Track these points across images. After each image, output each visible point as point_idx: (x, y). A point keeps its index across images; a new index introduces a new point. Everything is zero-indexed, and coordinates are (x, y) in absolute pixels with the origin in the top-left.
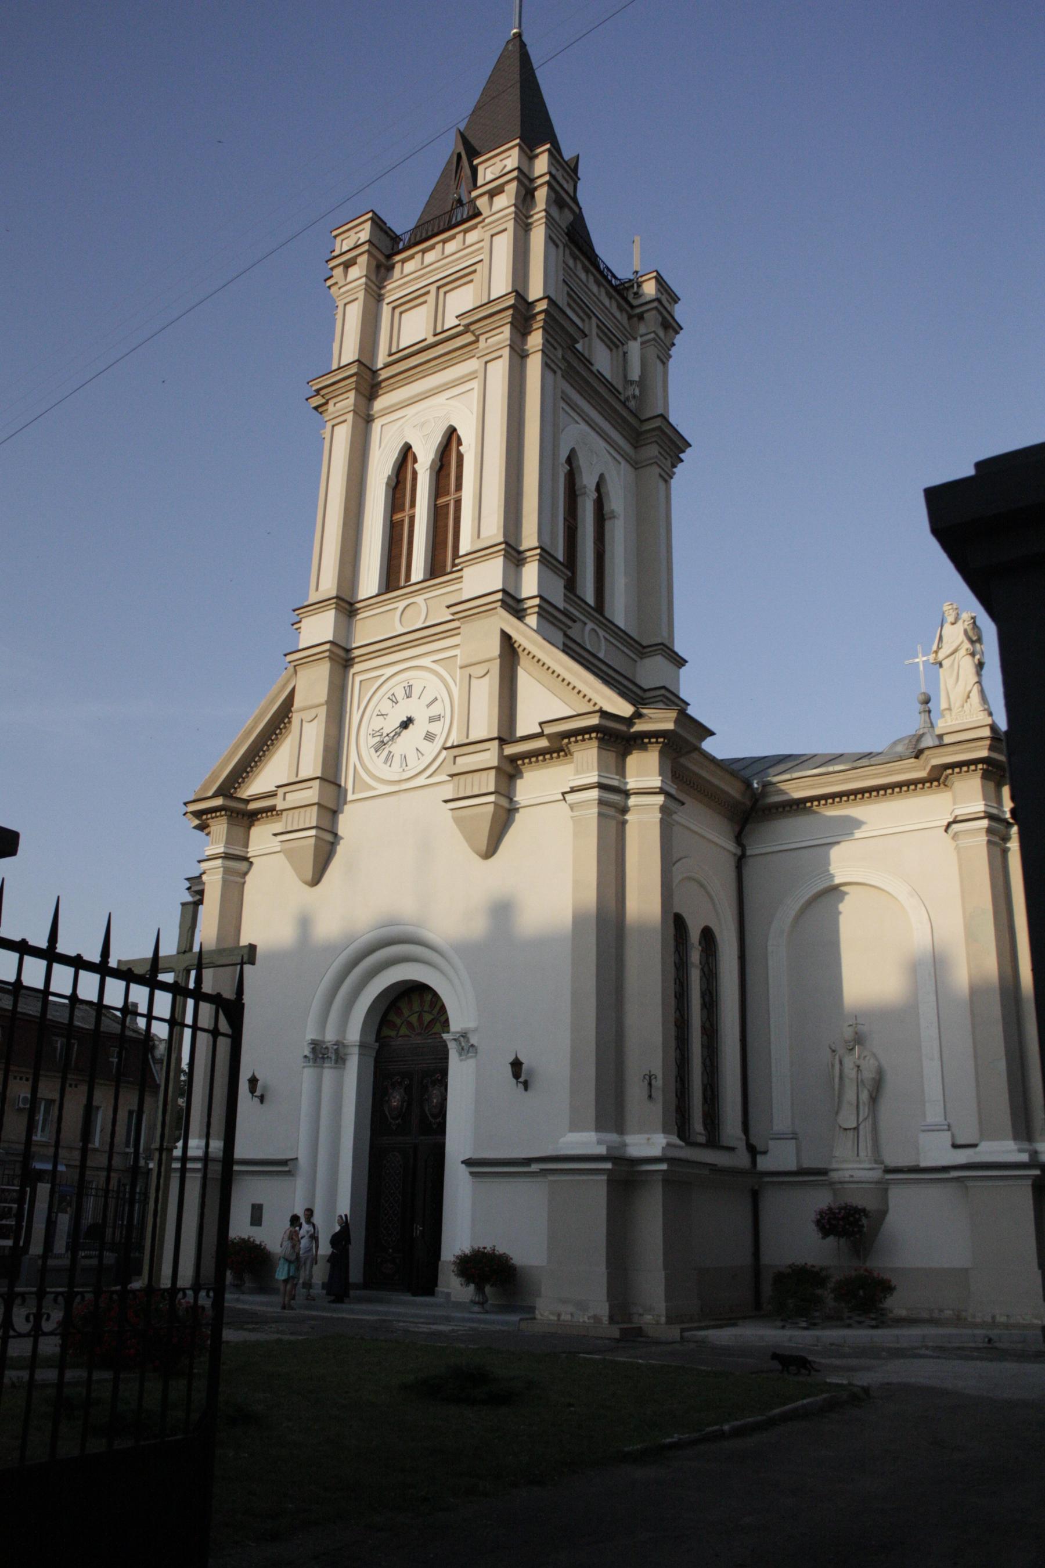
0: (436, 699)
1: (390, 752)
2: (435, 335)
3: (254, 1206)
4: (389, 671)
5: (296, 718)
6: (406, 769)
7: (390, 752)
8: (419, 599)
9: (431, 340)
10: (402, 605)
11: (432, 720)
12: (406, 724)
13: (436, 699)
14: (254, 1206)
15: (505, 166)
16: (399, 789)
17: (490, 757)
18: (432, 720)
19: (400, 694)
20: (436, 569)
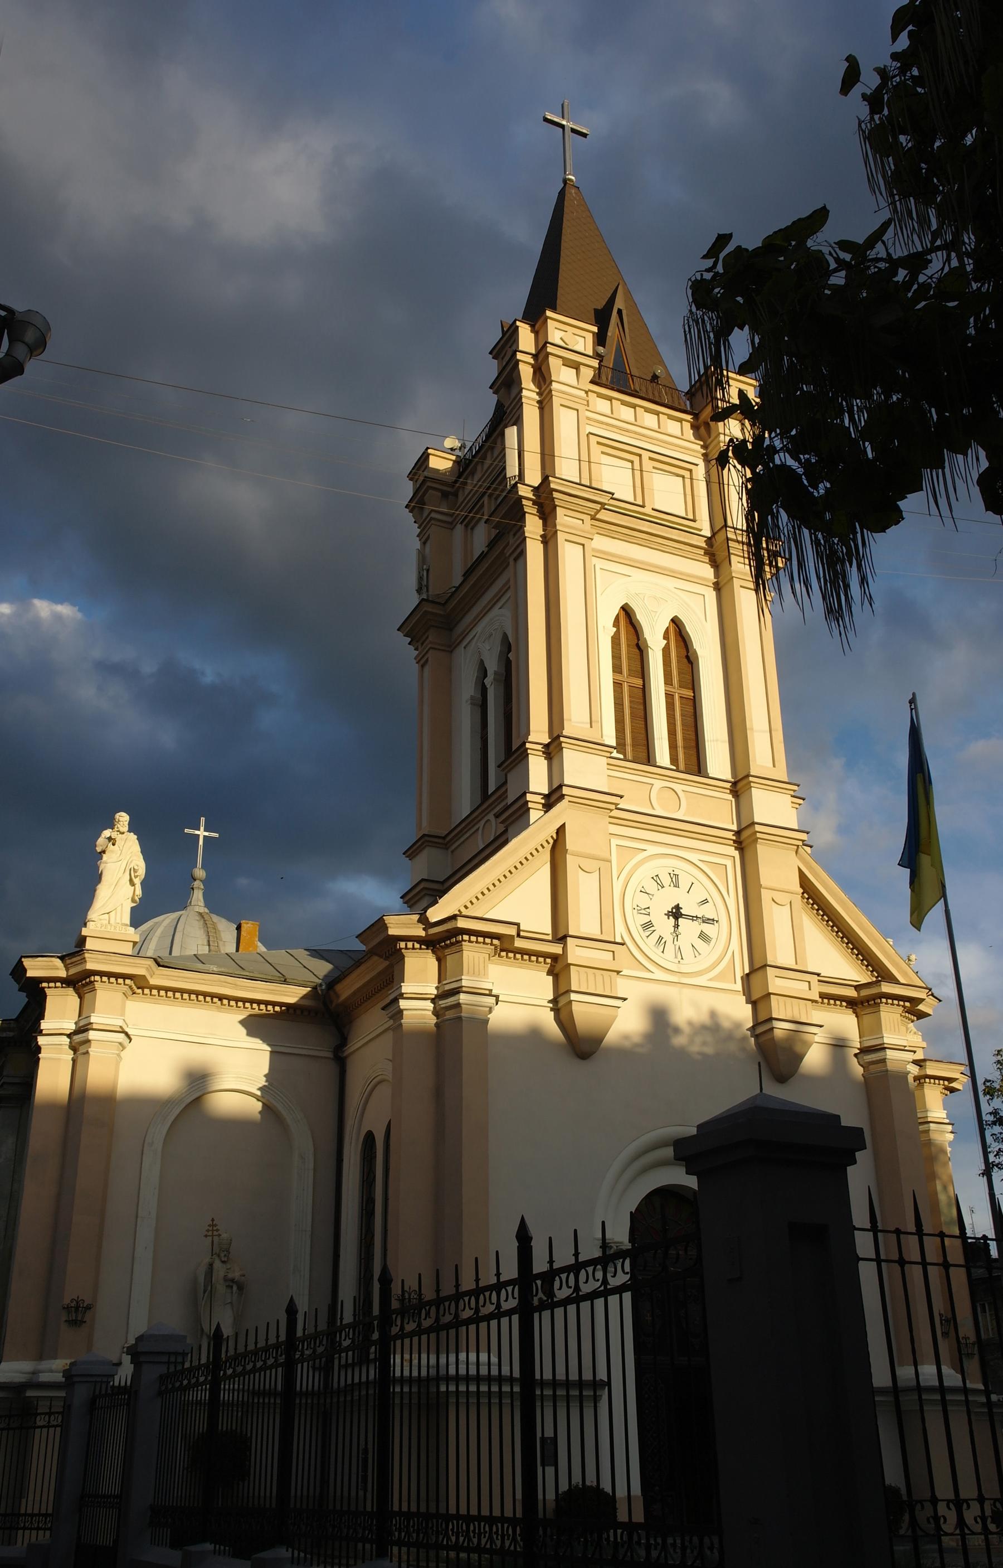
4: (653, 850)
7: (661, 938)
8: (678, 788)
10: (658, 784)
12: (676, 913)
19: (666, 880)
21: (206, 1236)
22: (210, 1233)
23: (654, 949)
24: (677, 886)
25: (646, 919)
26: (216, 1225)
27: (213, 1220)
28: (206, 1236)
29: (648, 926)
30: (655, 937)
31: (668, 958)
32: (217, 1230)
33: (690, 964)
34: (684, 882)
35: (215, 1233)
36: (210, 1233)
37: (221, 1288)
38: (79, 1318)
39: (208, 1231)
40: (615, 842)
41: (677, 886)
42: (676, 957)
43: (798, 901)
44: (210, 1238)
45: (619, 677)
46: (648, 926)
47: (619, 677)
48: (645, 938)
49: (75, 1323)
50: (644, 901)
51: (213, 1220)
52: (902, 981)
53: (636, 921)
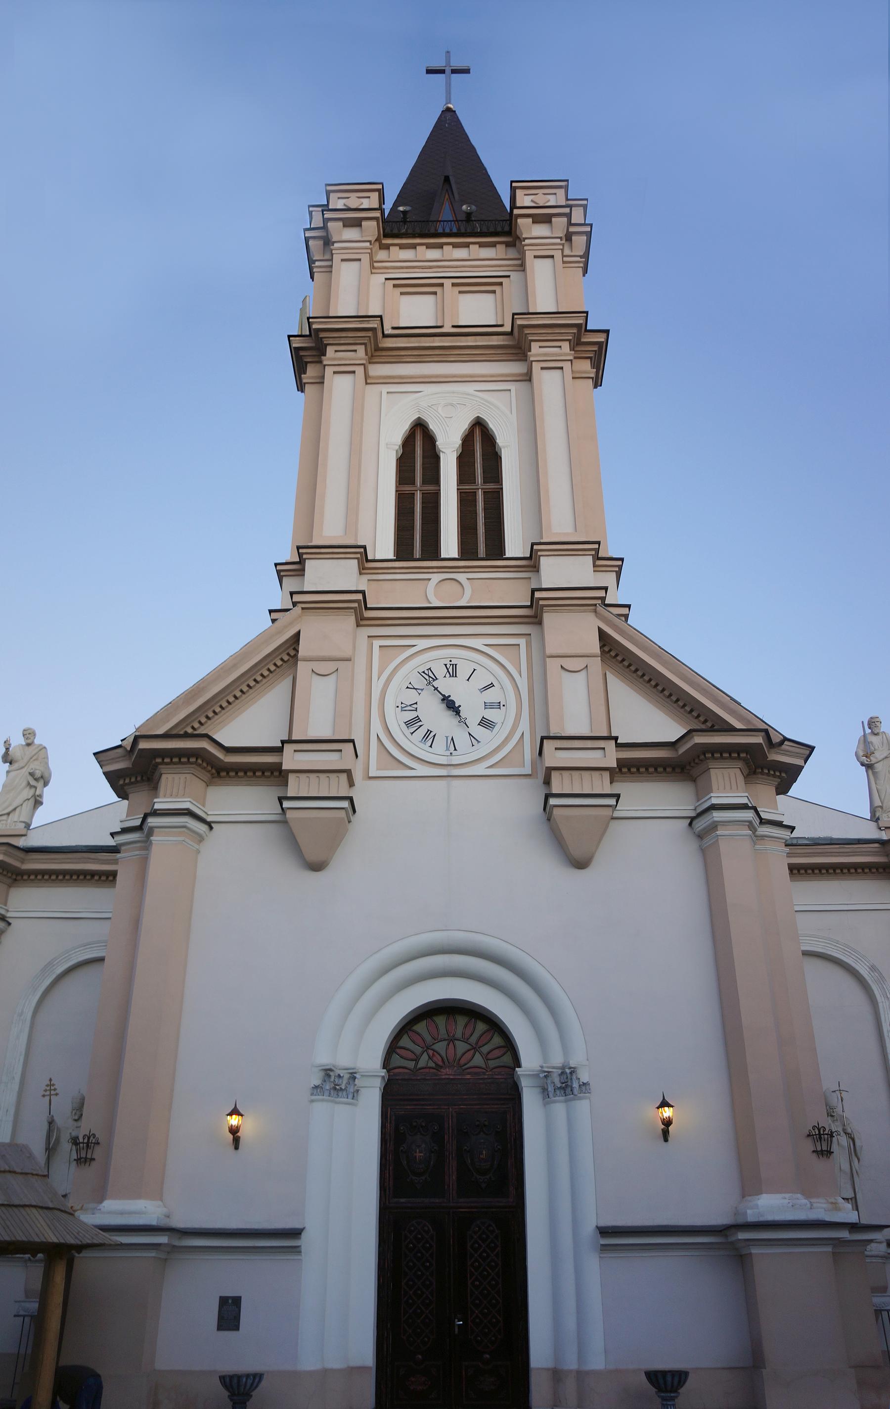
0: (492, 685)
1: (429, 732)
2: (453, 326)
3: (224, 1301)
4: (423, 644)
5: (303, 668)
6: (454, 753)
7: (429, 732)
8: (462, 577)
9: (447, 329)
10: (436, 578)
11: (487, 706)
13: (492, 685)
14: (224, 1301)
15: (549, 201)
16: (449, 774)
17: (610, 757)
18: (487, 706)
20: (467, 550)
21: (44, 1096)
22: (48, 1093)
23: (421, 745)
24: (454, 675)
25: (413, 715)
26: (53, 1085)
27: (51, 1080)
28: (44, 1096)
29: (414, 723)
30: (422, 732)
31: (438, 753)
32: (55, 1090)
33: (465, 752)
34: (464, 670)
35: (52, 1092)
36: (48, 1093)
37: (66, 1147)
38: (89, 1156)
39: (46, 1091)
40: (377, 643)
41: (454, 675)
42: (448, 749)
43: (596, 664)
44: (47, 1098)
45: (407, 488)
46: (414, 723)
47: (407, 488)
48: (409, 735)
49: (83, 1161)
50: (410, 697)
51: (51, 1080)
52: (738, 725)
53: (396, 720)
